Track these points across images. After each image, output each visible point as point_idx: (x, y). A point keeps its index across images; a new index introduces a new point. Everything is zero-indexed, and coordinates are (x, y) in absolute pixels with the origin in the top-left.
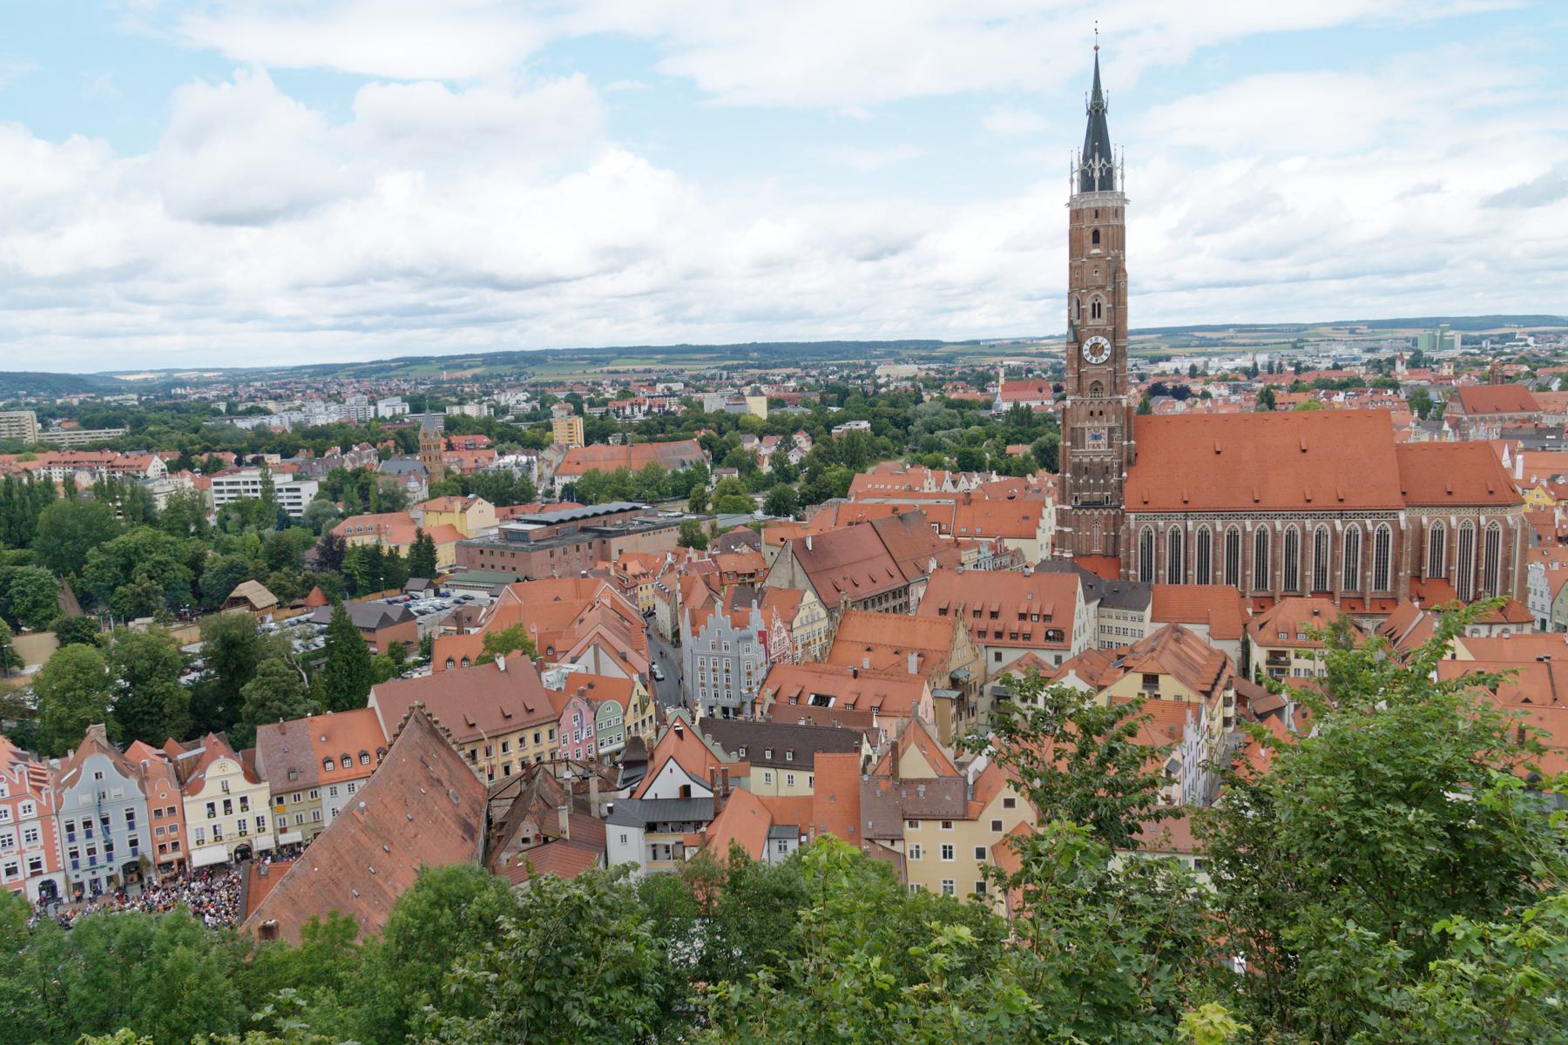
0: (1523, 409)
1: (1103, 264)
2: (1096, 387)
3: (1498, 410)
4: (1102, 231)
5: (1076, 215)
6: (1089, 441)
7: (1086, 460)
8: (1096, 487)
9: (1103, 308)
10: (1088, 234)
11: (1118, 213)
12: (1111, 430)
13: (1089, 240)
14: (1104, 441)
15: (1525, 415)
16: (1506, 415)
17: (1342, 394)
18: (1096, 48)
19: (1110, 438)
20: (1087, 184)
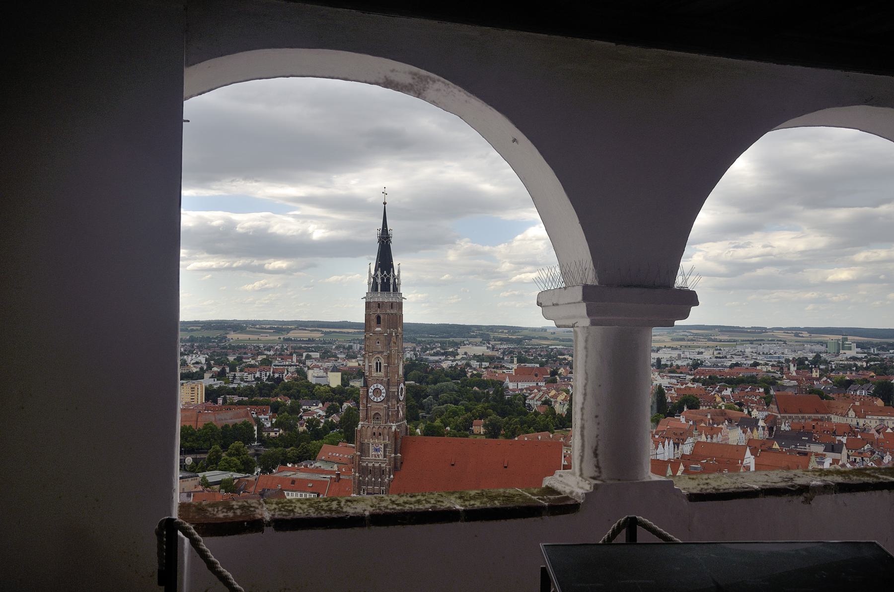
0: (817, 412)
1: (382, 338)
2: (377, 416)
3: (801, 412)
4: (382, 316)
5: (368, 305)
6: (372, 452)
7: (370, 465)
8: (375, 484)
9: (382, 365)
10: (374, 317)
11: (400, 305)
12: (385, 446)
13: (374, 323)
14: (382, 453)
15: (819, 416)
16: (807, 416)
17: (729, 390)
18: (385, 203)
19: (385, 451)
20: (374, 288)
